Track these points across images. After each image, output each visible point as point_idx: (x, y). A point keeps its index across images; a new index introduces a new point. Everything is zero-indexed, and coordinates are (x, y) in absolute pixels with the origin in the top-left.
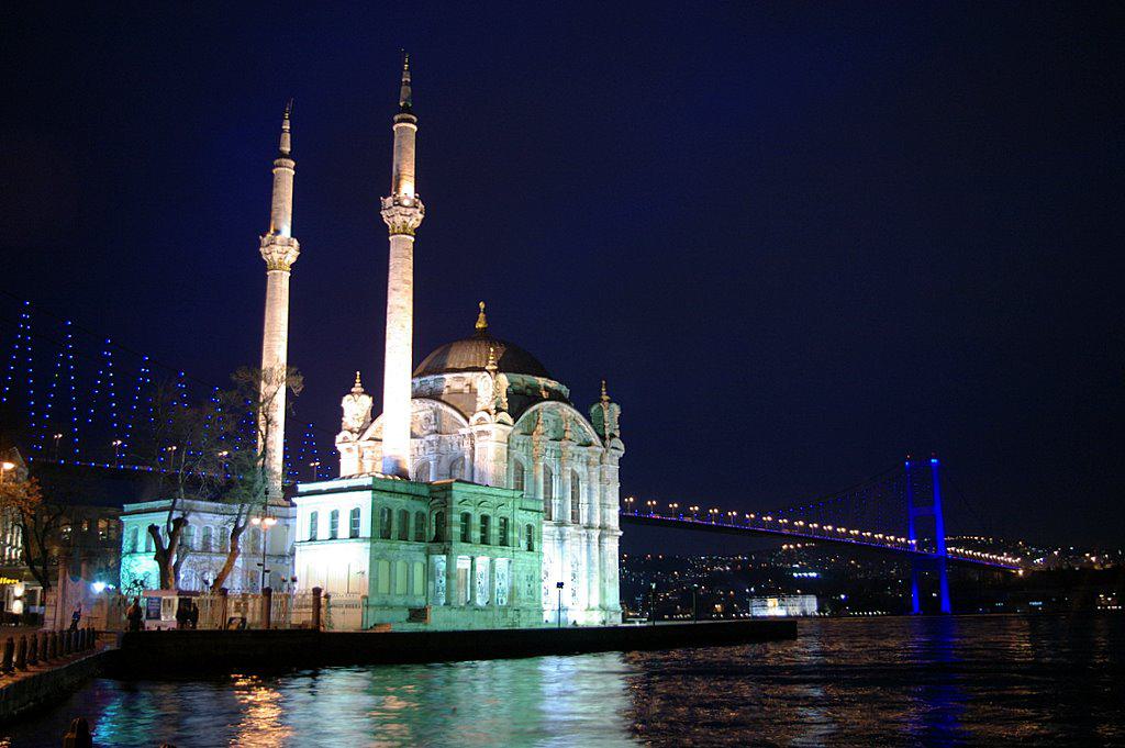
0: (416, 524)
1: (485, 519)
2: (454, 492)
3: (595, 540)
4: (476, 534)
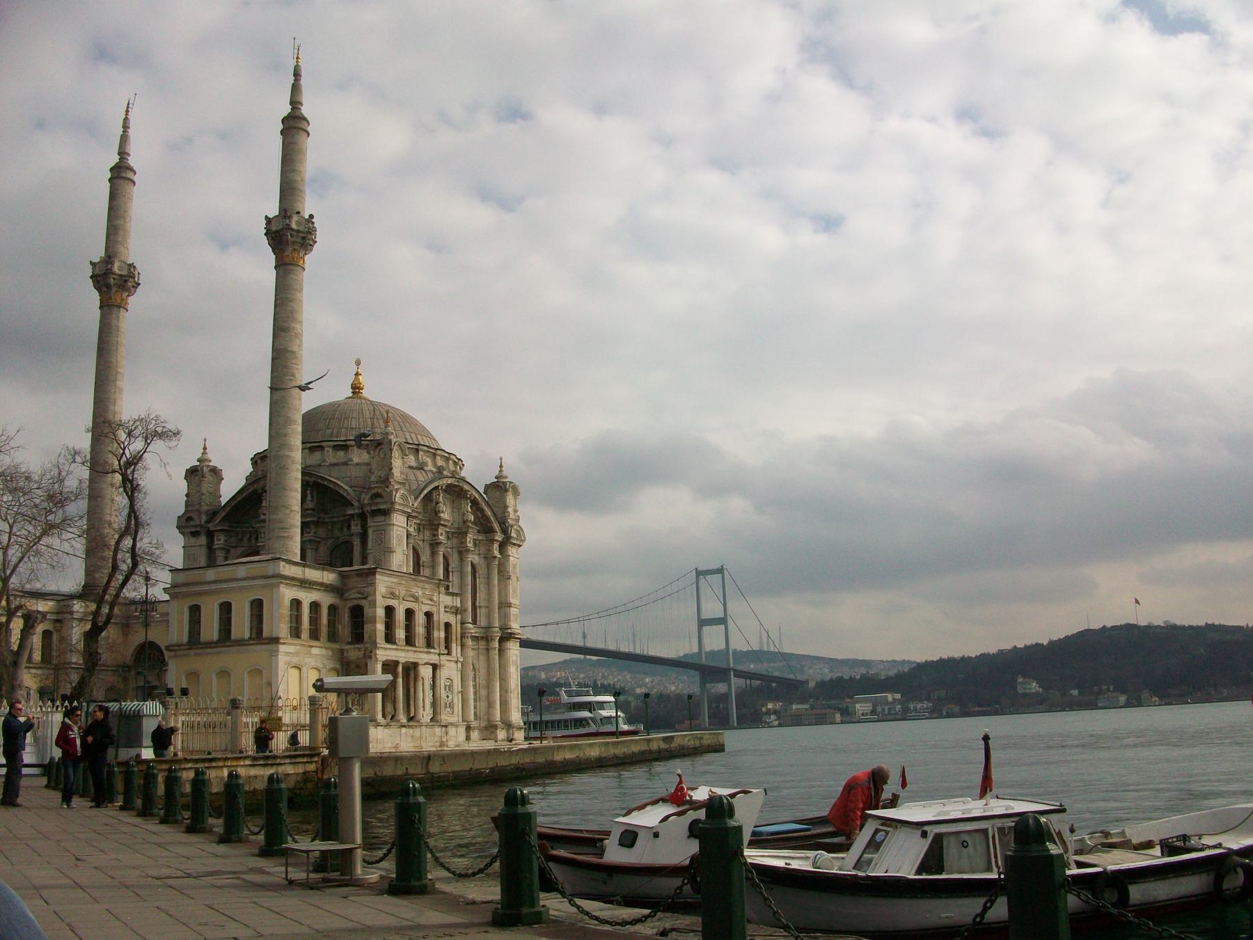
0: (329, 620)
1: (409, 613)
3: (496, 644)
4: (400, 634)
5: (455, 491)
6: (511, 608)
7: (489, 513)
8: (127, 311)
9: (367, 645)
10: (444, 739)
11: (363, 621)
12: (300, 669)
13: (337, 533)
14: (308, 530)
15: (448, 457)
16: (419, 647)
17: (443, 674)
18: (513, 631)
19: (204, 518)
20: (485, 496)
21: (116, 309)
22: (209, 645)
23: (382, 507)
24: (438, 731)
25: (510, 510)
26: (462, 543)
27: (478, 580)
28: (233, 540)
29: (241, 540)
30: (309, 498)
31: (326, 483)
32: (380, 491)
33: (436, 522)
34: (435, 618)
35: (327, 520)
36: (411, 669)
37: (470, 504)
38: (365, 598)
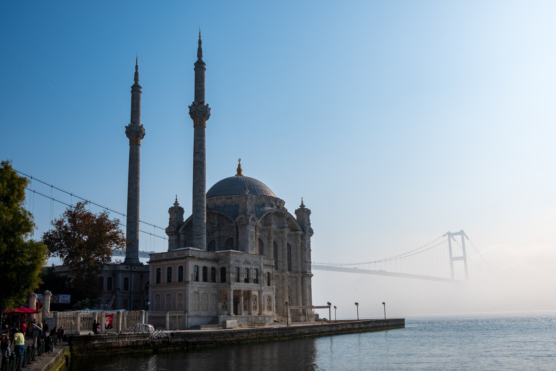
4: (242, 278)
7: (295, 222)
8: (140, 145)
27: (292, 251)
31: (222, 214)
34: (259, 271)
36: (248, 294)
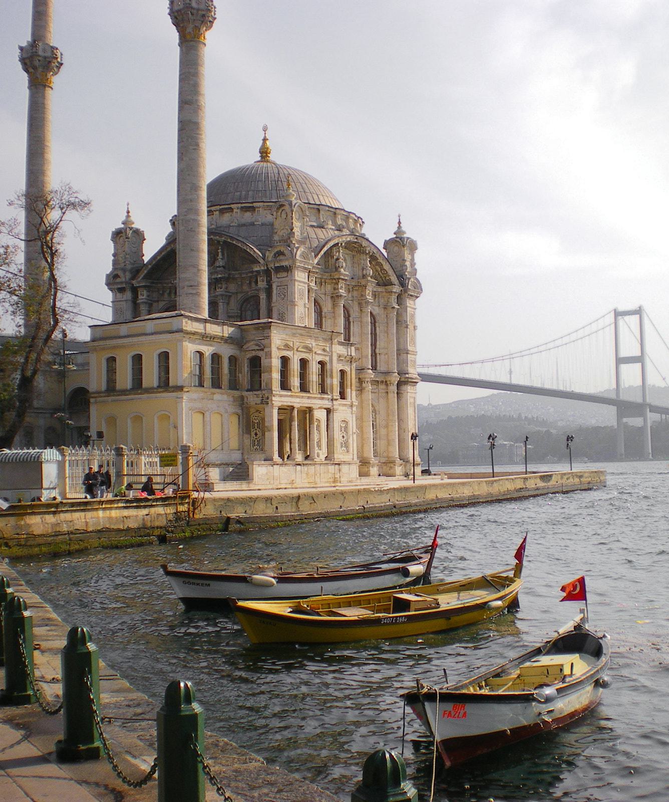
1: (304, 363)
2: (272, 334)
3: (394, 388)
4: (295, 381)
5: (355, 248)
6: (409, 355)
9: (264, 392)
10: (337, 476)
11: (261, 370)
12: (204, 414)
13: (245, 288)
14: (219, 286)
15: (348, 215)
16: (313, 394)
17: (337, 417)
18: (410, 376)
19: (128, 275)
20: (384, 251)
21: (41, 88)
22: (124, 392)
23: (284, 264)
24: (332, 468)
25: (408, 264)
26: (362, 295)
27: (377, 328)
28: (155, 295)
29: (163, 294)
30: (220, 256)
32: (282, 249)
33: (336, 277)
34: (328, 366)
35: (236, 276)
36: (307, 413)
37: (369, 259)
38: (263, 350)
